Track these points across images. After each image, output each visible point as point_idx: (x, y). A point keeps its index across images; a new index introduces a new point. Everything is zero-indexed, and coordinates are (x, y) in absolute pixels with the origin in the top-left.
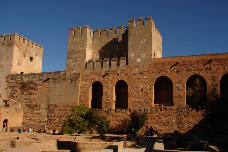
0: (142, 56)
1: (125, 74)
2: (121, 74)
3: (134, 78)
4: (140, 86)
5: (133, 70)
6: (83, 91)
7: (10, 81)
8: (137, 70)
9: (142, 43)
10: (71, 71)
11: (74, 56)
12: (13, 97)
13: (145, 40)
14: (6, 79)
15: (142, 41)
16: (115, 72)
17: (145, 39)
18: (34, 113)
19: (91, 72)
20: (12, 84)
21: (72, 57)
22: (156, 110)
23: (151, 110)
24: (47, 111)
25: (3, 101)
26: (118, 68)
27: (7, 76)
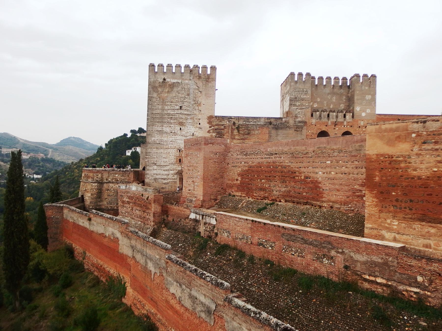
0: (367, 111)
1: (351, 126)
2: (347, 126)
3: (360, 130)
5: (359, 123)
7: (214, 123)
10: (295, 119)
11: (298, 104)
14: (207, 120)
16: (342, 123)
19: (318, 121)
20: (216, 127)
21: (296, 104)
26: (345, 120)
27: (208, 117)
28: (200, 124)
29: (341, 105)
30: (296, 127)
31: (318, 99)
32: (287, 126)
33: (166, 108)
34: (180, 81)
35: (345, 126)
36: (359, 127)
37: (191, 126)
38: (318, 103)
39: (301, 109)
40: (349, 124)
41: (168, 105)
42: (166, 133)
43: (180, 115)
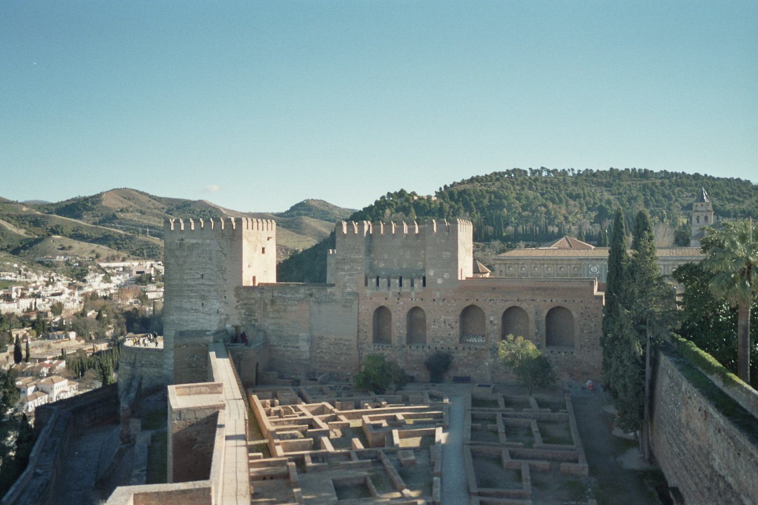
0: (445, 276)
1: (422, 299)
11: (346, 267)
12: (251, 321)
13: (449, 254)
16: (408, 295)
18: (288, 347)
20: (245, 301)
22: (464, 349)
23: (456, 348)
24: (309, 344)
25: (233, 326)
26: (412, 290)
28: (225, 297)
33: (185, 277)
34: (200, 242)
37: (215, 301)
41: (188, 273)
42: (186, 310)
43: (202, 287)
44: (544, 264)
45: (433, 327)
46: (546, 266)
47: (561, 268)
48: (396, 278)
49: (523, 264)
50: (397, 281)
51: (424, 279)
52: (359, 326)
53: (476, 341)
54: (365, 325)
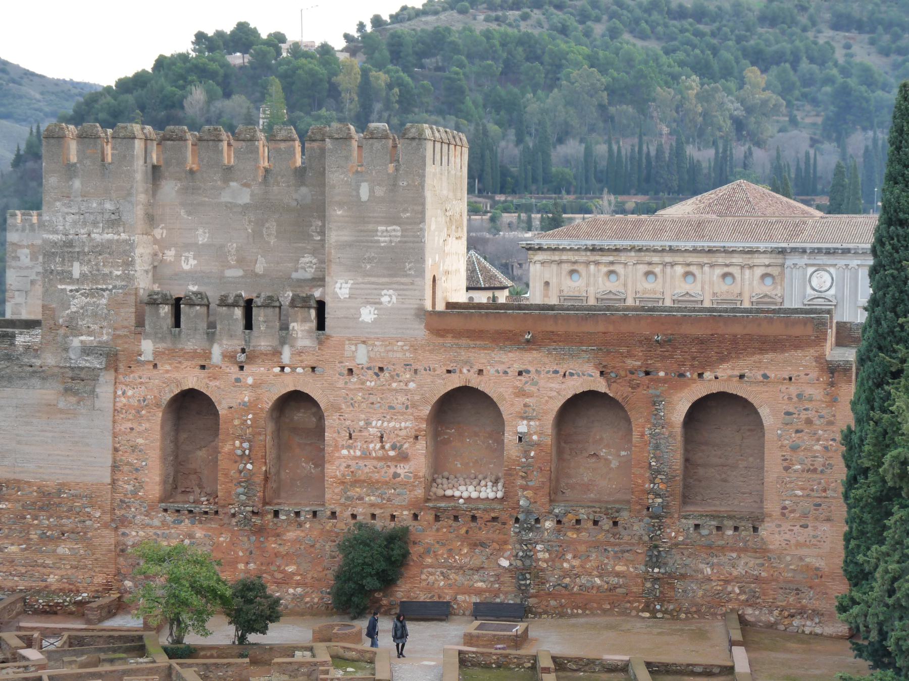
0: (385, 299)
1: (313, 369)
2: (294, 369)
4: (374, 423)
6: (132, 429)
8: (362, 355)
9: (383, 240)
11: (77, 270)
13: (396, 230)
15: (383, 232)
17: (398, 228)
29: (302, 260)
30: (70, 374)
31: (200, 231)
32: (35, 372)
35: (287, 370)
36: (350, 371)
38: (199, 250)
39: (91, 294)
40: (302, 361)
44: (673, 265)
45: (345, 452)
46: (680, 270)
47: (725, 276)
48: (235, 305)
49: (612, 263)
50: (238, 313)
51: (321, 307)
52: (116, 450)
53: (474, 495)
54: (134, 448)
